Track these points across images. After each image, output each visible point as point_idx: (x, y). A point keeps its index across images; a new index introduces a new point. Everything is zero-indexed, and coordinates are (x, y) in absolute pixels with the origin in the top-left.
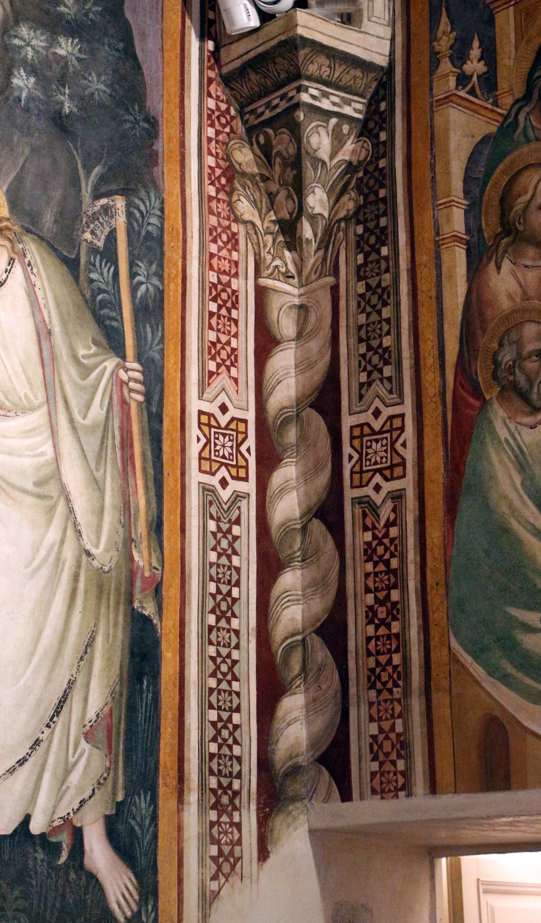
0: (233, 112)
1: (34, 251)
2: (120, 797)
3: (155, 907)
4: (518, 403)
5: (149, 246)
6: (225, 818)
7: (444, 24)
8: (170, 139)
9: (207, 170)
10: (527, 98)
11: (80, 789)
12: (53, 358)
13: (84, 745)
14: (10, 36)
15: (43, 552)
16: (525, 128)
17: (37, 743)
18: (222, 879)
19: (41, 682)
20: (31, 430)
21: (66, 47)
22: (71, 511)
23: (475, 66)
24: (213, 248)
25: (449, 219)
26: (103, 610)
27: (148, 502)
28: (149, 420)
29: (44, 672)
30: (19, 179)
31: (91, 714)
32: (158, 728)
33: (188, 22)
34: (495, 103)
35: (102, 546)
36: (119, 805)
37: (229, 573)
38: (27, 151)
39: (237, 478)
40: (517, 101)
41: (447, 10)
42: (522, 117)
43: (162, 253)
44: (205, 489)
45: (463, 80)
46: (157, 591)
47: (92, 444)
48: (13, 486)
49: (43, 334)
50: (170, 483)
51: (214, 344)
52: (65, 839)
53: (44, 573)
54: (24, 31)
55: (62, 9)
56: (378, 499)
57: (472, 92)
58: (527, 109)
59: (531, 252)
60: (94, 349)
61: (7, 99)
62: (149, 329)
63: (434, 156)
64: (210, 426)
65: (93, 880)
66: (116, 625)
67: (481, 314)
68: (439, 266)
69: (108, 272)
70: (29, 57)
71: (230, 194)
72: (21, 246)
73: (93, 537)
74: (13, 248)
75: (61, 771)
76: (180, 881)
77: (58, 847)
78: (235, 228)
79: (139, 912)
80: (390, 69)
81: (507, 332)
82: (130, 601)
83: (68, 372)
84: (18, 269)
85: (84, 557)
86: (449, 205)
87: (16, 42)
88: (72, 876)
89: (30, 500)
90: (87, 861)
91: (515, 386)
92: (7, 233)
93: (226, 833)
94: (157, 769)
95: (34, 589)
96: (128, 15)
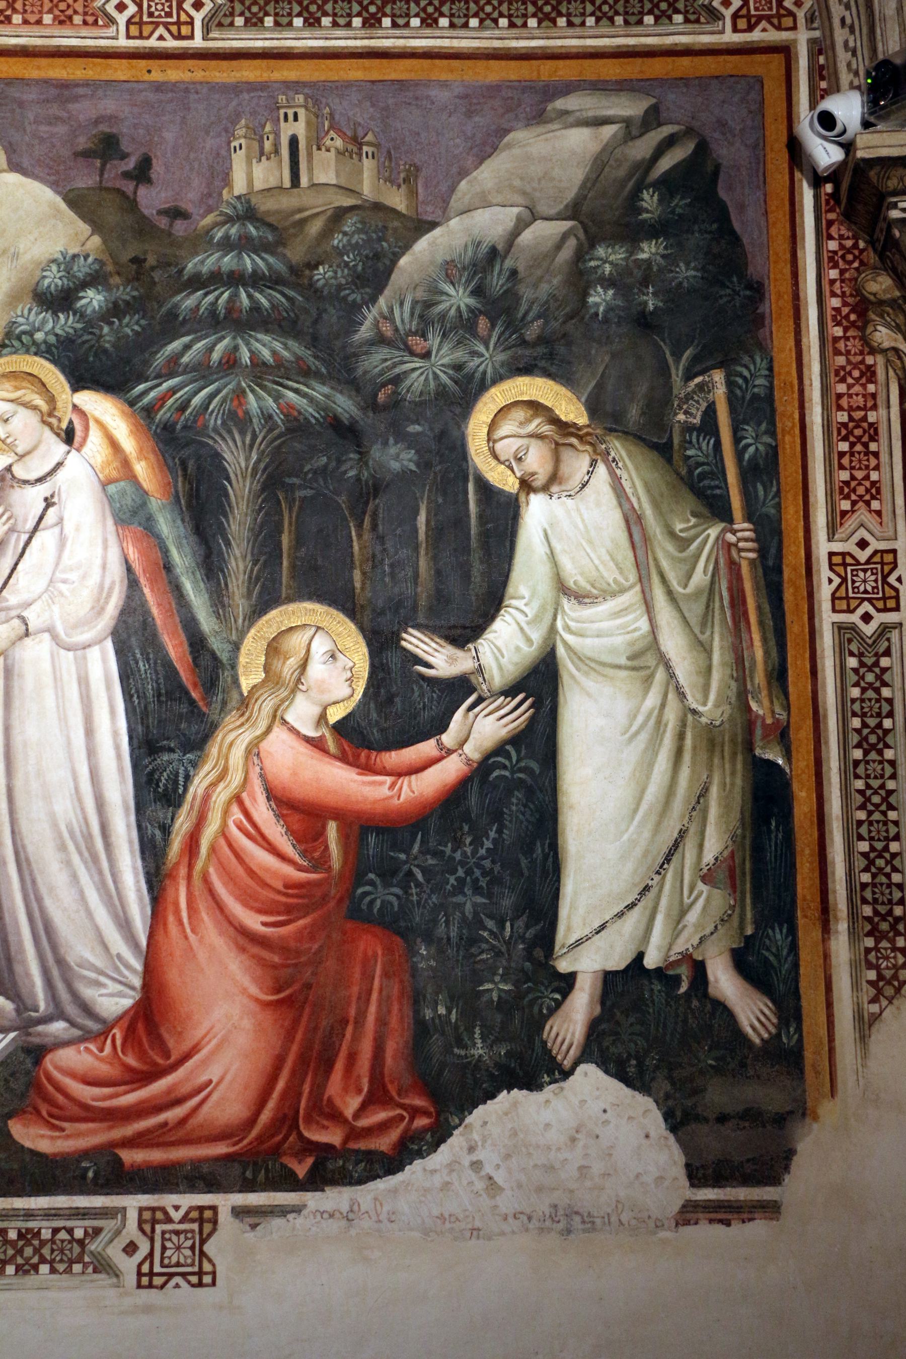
0: (862, 244)
1: (617, 447)
2: (749, 931)
3: (799, 1029)
5: (756, 408)
6: (884, 944)
8: (780, 296)
9: (829, 313)
11: (699, 926)
12: (646, 539)
13: (701, 886)
14: (585, 261)
15: (640, 719)
17: (647, 888)
18: (884, 1002)
19: (647, 834)
20: (621, 611)
21: (648, 250)
22: (672, 675)
24: (841, 388)
26: (716, 761)
27: (767, 653)
28: (765, 574)
29: (650, 826)
30: (600, 386)
31: (708, 857)
32: (793, 865)
33: (798, 175)
35: (710, 704)
36: (749, 940)
37: (877, 705)
38: (607, 358)
39: (886, 610)
43: (773, 411)
44: (840, 628)
46: (782, 735)
47: (694, 611)
48: (604, 664)
49: (632, 521)
50: (795, 627)
51: (847, 483)
52: (684, 972)
53: (644, 736)
54: (601, 251)
55: (645, 216)
60: (693, 521)
61: (583, 318)
62: (760, 487)
64: (845, 565)
65: (721, 1008)
66: (733, 773)
69: (707, 445)
70: (607, 273)
71: (862, 329)
72: (603, 446)
73: (699, 696)
74: (595, 451)
75: (675, 912)
76: (829, 1005)
77: (677, 979)
78: (870, 360)
79: (779, 1035)
82: (749, 747)
83: (664, 550)
84: (601, 469)
85: (690, 717)
87: (593, 263)
88: (695, 1003)
89: (623, 674)
90: (711, 990)
92: (589, 438)
93: (887, 958)
94: (794, 902)
95: (633, 753)
96: (722, 194)
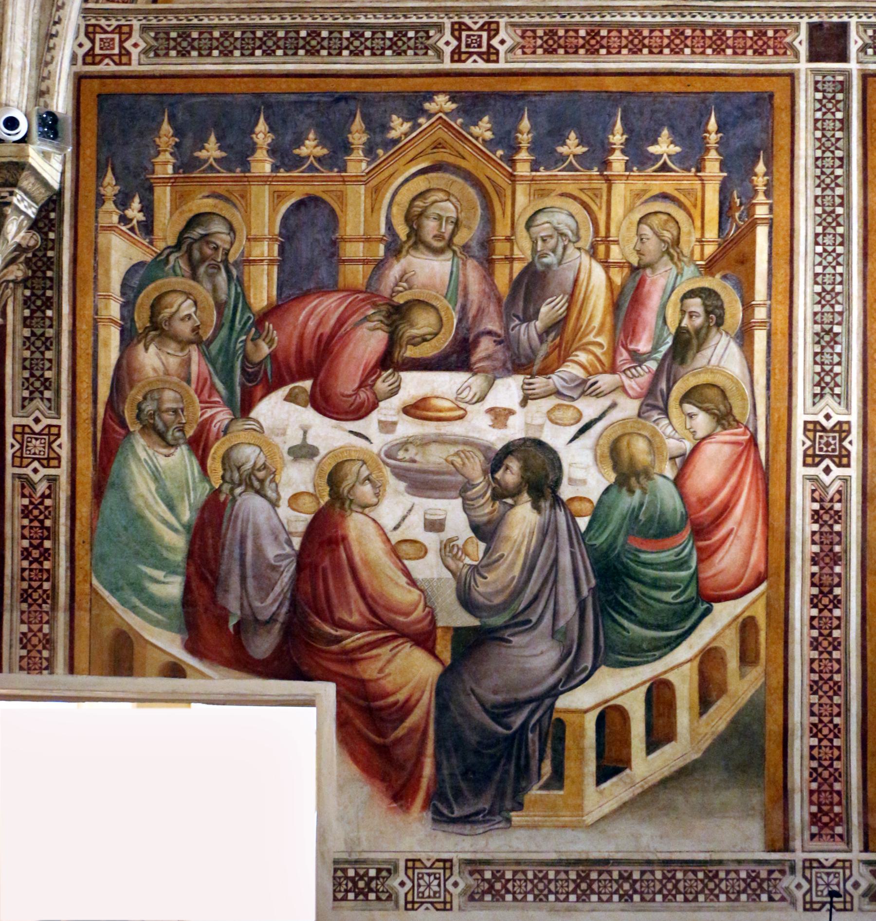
4: (155, 437)
7: (109, 178)
10: (177, 247)
16: (174, 266)
23: (135, 212)
25: (107, 307)
34: (151, 243)
40: (169, 247)
41: (113, 170)
42: (172, 258)
45: (124, 219)
56: (36, 478)
57: (132, 229)
58: (177, 255)
59: (173, 345)
63: (96, 261)
67: (130, 374)
68: (96, 335)
80: (60, 193)
81: (151, 391)
86: (107, 297)
91: (154, 427)
